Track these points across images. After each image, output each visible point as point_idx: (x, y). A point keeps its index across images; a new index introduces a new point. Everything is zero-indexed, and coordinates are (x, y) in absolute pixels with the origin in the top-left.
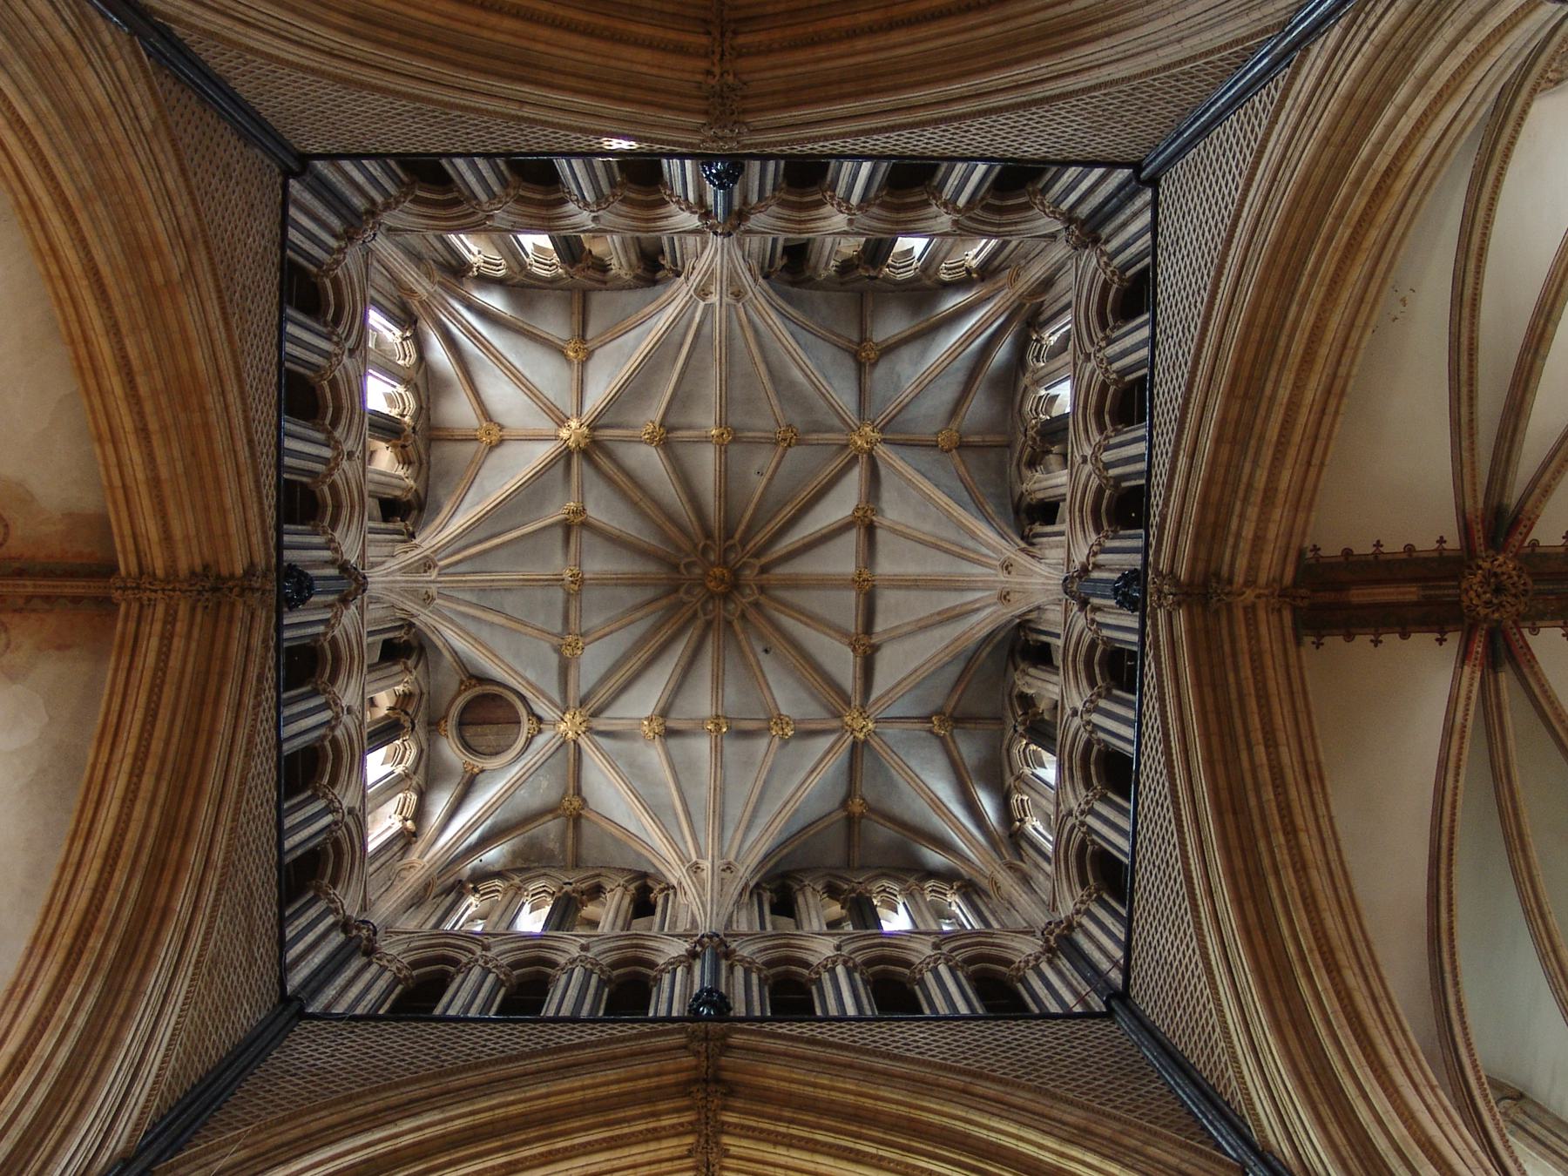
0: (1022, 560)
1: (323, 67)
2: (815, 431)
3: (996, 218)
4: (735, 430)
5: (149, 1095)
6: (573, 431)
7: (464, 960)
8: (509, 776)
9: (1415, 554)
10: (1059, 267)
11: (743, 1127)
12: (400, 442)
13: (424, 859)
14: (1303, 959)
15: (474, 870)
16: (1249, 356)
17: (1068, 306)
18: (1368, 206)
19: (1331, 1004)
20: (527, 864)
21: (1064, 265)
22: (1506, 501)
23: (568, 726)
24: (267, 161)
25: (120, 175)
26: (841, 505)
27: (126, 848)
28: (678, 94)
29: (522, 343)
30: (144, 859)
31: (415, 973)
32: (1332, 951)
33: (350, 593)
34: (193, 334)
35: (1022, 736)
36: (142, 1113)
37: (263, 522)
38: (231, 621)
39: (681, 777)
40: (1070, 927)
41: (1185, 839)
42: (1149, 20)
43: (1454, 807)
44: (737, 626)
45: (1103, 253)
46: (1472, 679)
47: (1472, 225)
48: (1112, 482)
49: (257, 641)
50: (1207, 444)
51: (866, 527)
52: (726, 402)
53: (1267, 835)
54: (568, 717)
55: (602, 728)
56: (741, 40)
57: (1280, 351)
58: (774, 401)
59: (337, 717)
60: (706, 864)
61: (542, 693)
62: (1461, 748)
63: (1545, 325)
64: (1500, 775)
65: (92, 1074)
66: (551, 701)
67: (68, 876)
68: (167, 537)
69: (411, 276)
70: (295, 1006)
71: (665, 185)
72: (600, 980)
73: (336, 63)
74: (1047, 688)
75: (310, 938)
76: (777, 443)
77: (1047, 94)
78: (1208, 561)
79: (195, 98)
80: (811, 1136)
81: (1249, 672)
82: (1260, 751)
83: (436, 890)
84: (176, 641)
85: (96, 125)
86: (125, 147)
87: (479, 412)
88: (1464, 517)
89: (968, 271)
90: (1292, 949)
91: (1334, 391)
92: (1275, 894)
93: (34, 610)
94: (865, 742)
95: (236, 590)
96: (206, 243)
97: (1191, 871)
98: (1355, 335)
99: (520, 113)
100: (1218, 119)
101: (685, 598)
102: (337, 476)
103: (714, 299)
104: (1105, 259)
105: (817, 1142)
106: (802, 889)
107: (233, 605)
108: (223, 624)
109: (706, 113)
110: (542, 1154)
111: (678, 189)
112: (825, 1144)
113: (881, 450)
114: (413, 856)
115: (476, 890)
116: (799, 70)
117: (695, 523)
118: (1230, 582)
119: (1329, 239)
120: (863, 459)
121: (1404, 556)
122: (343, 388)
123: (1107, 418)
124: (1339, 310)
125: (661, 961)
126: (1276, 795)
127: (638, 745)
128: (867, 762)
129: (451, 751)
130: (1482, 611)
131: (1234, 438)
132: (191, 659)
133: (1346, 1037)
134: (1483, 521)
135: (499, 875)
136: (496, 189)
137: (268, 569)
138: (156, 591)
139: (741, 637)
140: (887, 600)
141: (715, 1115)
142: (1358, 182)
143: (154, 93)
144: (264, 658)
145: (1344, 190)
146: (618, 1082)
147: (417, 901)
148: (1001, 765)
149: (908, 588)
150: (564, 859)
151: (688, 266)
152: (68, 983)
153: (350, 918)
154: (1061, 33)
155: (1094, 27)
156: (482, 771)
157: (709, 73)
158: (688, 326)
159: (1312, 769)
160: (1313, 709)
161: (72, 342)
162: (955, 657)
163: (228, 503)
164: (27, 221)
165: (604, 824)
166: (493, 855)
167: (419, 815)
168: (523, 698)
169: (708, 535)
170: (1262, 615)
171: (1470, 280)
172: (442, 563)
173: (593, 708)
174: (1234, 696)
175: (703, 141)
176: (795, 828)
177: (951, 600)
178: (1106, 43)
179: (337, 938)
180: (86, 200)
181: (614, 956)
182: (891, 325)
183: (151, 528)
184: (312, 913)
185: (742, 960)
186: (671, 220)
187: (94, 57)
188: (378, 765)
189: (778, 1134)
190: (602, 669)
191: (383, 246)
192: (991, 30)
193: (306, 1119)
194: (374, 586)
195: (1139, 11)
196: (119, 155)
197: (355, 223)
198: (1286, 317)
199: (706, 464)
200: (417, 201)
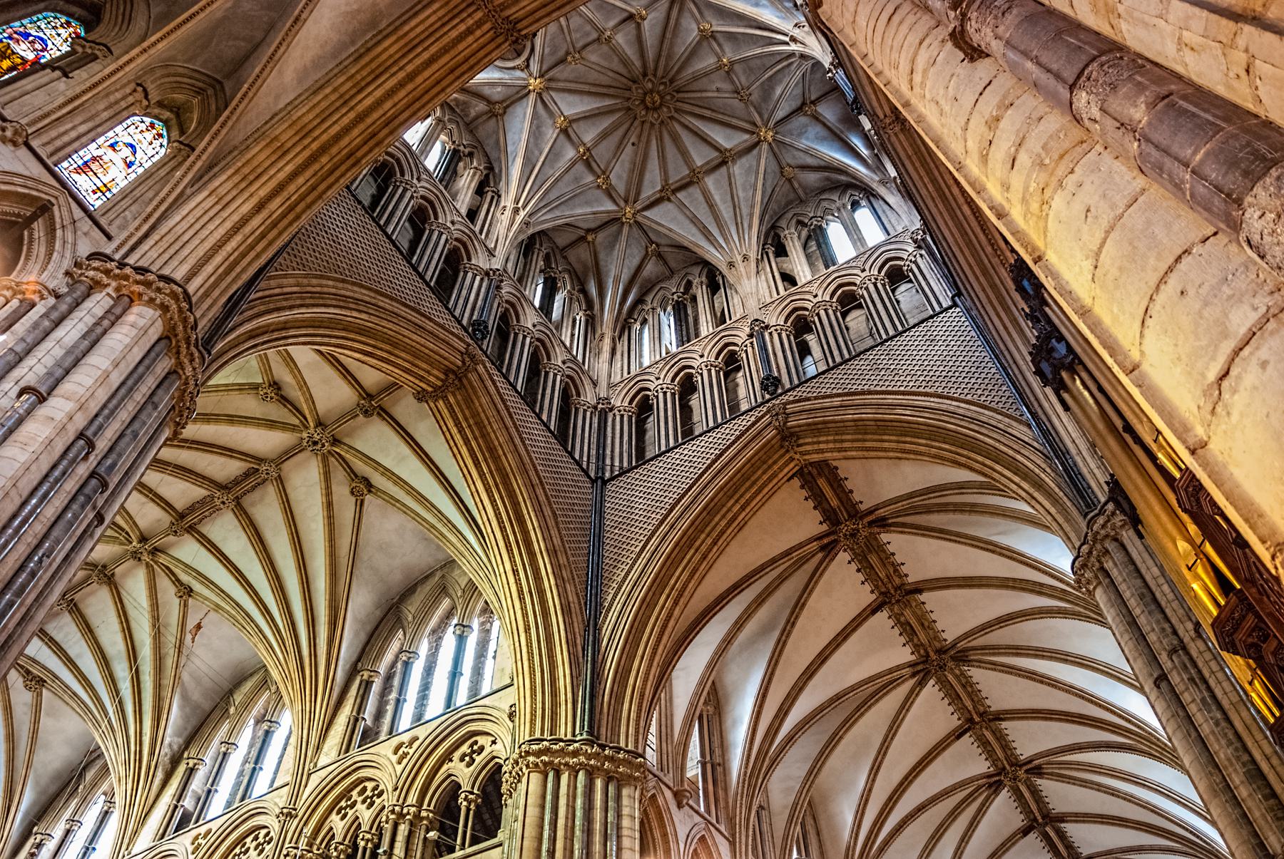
0: (753, 265)
2: (755, 107)
14: (672, 589)
26: (726, 139)
51: (724, 159)
53: (708, 536)
61: (542, 61)
64: (782, 579)
82: (738, 507)
90: (672, 582)
92: (688, 557)
101: (634, 89)
113: (765, 146)
118: (799, 446)
119: (958, 454)
120: (754, 138)
123: (840, 291)
125: (473, 262)
127: (550, 122)
140: (695, 191)
199: (706, 62)
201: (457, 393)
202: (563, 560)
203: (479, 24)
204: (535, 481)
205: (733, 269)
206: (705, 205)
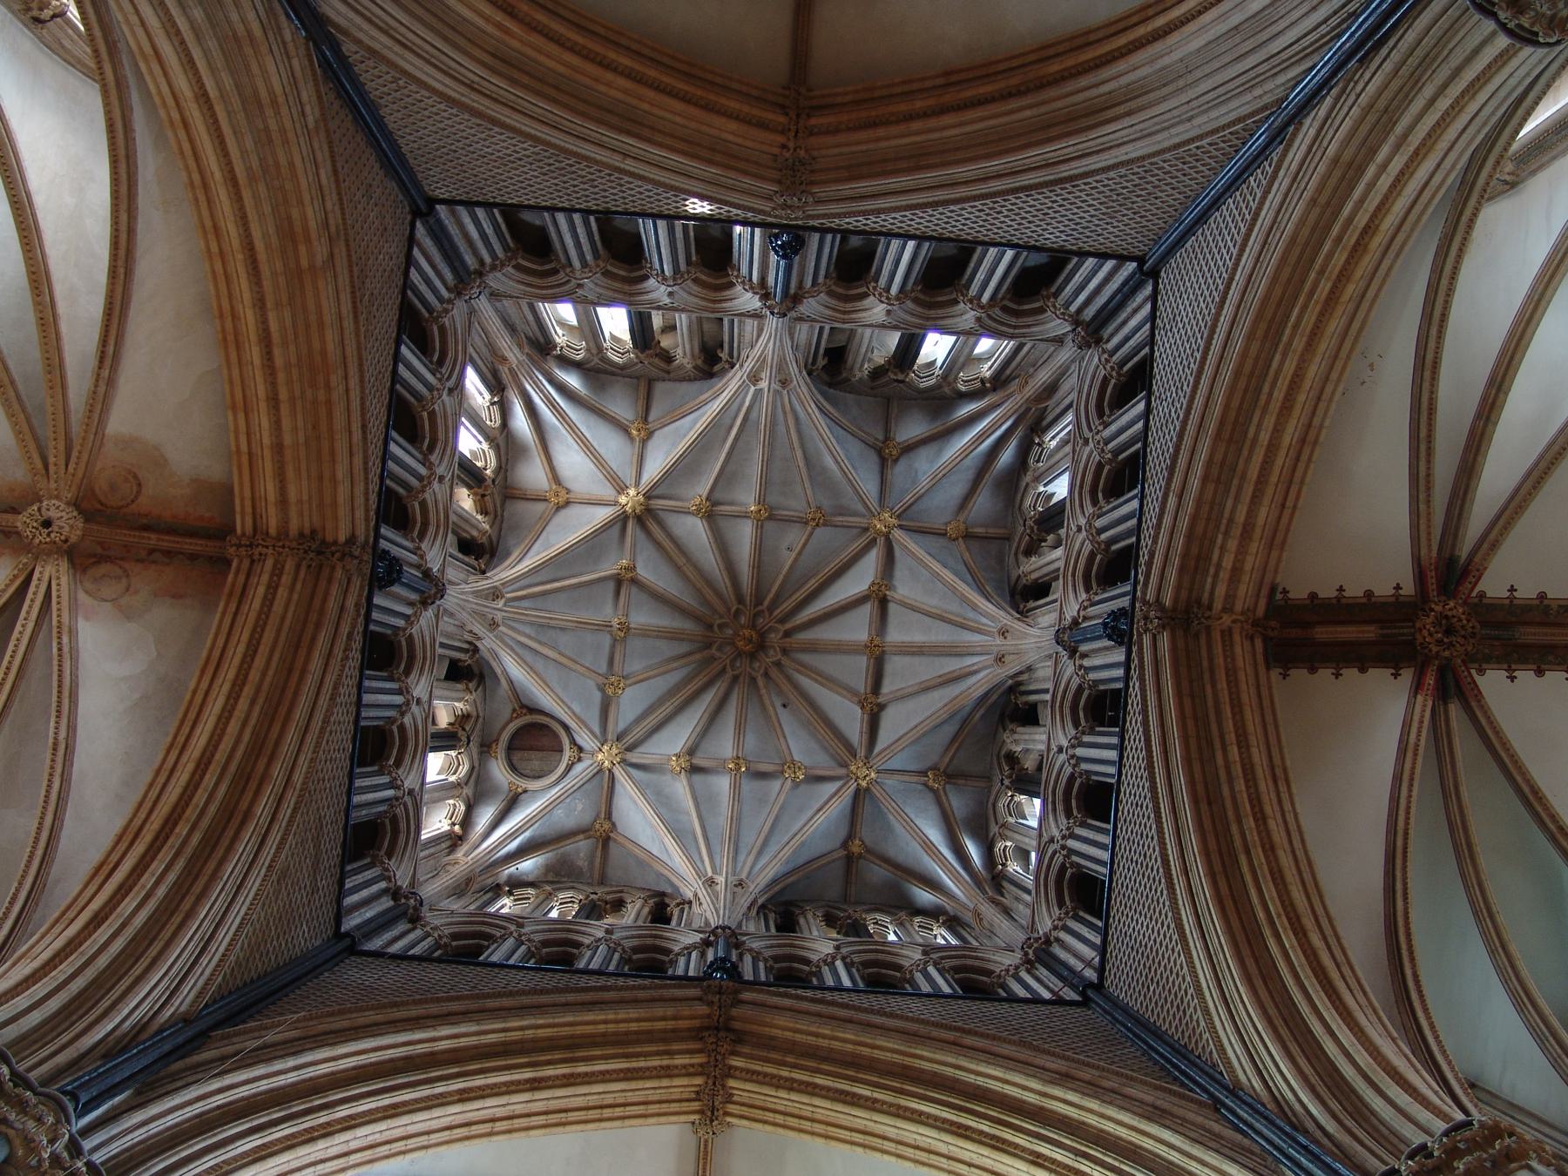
0: (1019, 626)
1: (463, 99)
2: (841, 515)
3: (1013, 321)
4: (771, 508)
5: (215, 970)
6: (630, 499)
7: (498, 934)
8: (548, 796)
9: (1373, 599)
10: (1063, 372)
11: (748, 1071)
12: (481, 491)
13: (465, 859)
15: (510, 876)
16: (1235, 404)
17: (1070, 406)
18: (1347, 262)
19: (1297, 958)
20: (557, 877)
21: (1068, 368)
22: (1457, 553)
23: (604, 757)
24: (401, 197)
25: (283, 160)
27: (217, 756)
28: (756, 163)
29: (593, 420)
30: (233, 768)
31: (454, 943)
32: (1298, 918)
33: (429, 597)
34: (327, 319)
35: (1008, 787)
36: (206, 984)
37: (367, 500)
38: (330, 581)
39: (702, 808)
40: (1048, 942)
41: (1163, 828)
42: (1165, 99)
43: (1408, 812)
44: (761, 682)
45: (1104, 351)
46: (1425, 706)
47: (1436, 294)
48: (1103, 546)
49: (350, 602)
50: (1195, 483)
51: (880, 600)
52: (765, 483)
53: (1239, 821)
54: (606, 748)
55: (634, 760)
56: (813, 121)
57: (1263, 397)
58: (807, 485)
59: (407, 703)
60: (721, 879)
62: (1414, 763)
63: (1497, 395)
65: (166, 938)
66: (592, 732)
67: (162, 779)
68: (283, 502)
69: (505, 344)
70: (347, 942)
71: (733, 268)
72: (621, 958)
73: (474, 96)
74: (1032, 743)
75: (365, 893)
76: (806, 523)
77: (1072, 172)
78: (1191, 590)
79: (350, 117)
80: (810, 1079)
81: (1225, 686)
82: (1234, 752)
83: (476, 887)
84: (281, 589)
85: (269, 112)
86: (291, 135)
87: (550, 476)
88: (1419, 565)
89: (983, 381)
90: (1261, 915)
91: (1308, 439)
92: (1245, 869)
93: (154, 562)
94: (867, 790)
95: (337, 555)
96: (347, 241)
97: (1167, 855)
98: (1329, 389)
99: (622, 166)
100: (1216, 204)
101: (718, 654)
102: (428, 495)
103: (764, 385)
104: (1106, 356)
105: (816, 1086)
106: (804, 913)
107: (333, 568)
108: (323, 584)
109: (779, 182)
110: (564, 1076)
111: (744, 270)
112: (823, 1088)
113: (897, 534)
114: (459, 854)
115: (510, 893)
116: (860, 148)
117: (730, 589)
118: (1210, 608)
120: (881, 541)
121: (1364, 600)
122: (439, 421)
124: (1317, 359)
125: (676, 949)
126: (1248, 788)
127: (667, 778)
128: (868, 808)
129: (499, 772)
130: (1435, 649)
131: (1219, 478)
132: (292, 608)
133: (1312, 985)
134: (1436, 569)
135: (532, 884)
136: (589, 257)
137: (367, 542)
138: (267, 547)
139: (763, 691)
140: (894, 665)
141: (723, 1059)
142: (1339, 239)
143: (319, 97)
144: (355, 620)
145: (1327, 247)
146: (638, 1020)
147: (461, 889)
148: (987, 820)
149: (913, 654)
150: (592, 877)
151: (743, 355)
152: (152, 860)
153: (400, 887)
154: (1086, 115)
155: (1117, 109)
156: (525, 791)
157: (784, 146)
158: (739, 410)
159: (1279, 772)
160: (1281, 723)
161: (221, 316)
162: (952, 717)
163: (340, 475)
164: (196, 200)
165: (630, 846)
166: (528, 865)
167: (467, 822)
168: (566, 728)
169: (740, 600)
170: (1237, 638)
171: (1432, 344)
172: (508, 595)
173: (629, 743)
174: (1210, 703)
175: (774, 209)
176: (801, 861)
177: (953, 665)
178: (1127, 122)
179: (386, 903)
180: (252, 178)
181: (635, 942)
182: (912, 428)
183: (270, 489)
184: (369, 874)
185: (750, 950)
186: (736, 302)
187: (275, 48)
188: (436, 765)
189: (781, 1077)
190: (639, 710)
191: (483, 304)
192: (1028, 113)
193: (354, 1015)
194: (450, 598)
195: (1158, 92)
196: (286, 142)
197: (465, 279)
198: (1269, 366)
200: (518, 267)
201: (739, 1048)
202: (1087, 1074)
203: (278, 571)
204: (950, 1035)
205: (1007, 659)
206: (916, 660)
